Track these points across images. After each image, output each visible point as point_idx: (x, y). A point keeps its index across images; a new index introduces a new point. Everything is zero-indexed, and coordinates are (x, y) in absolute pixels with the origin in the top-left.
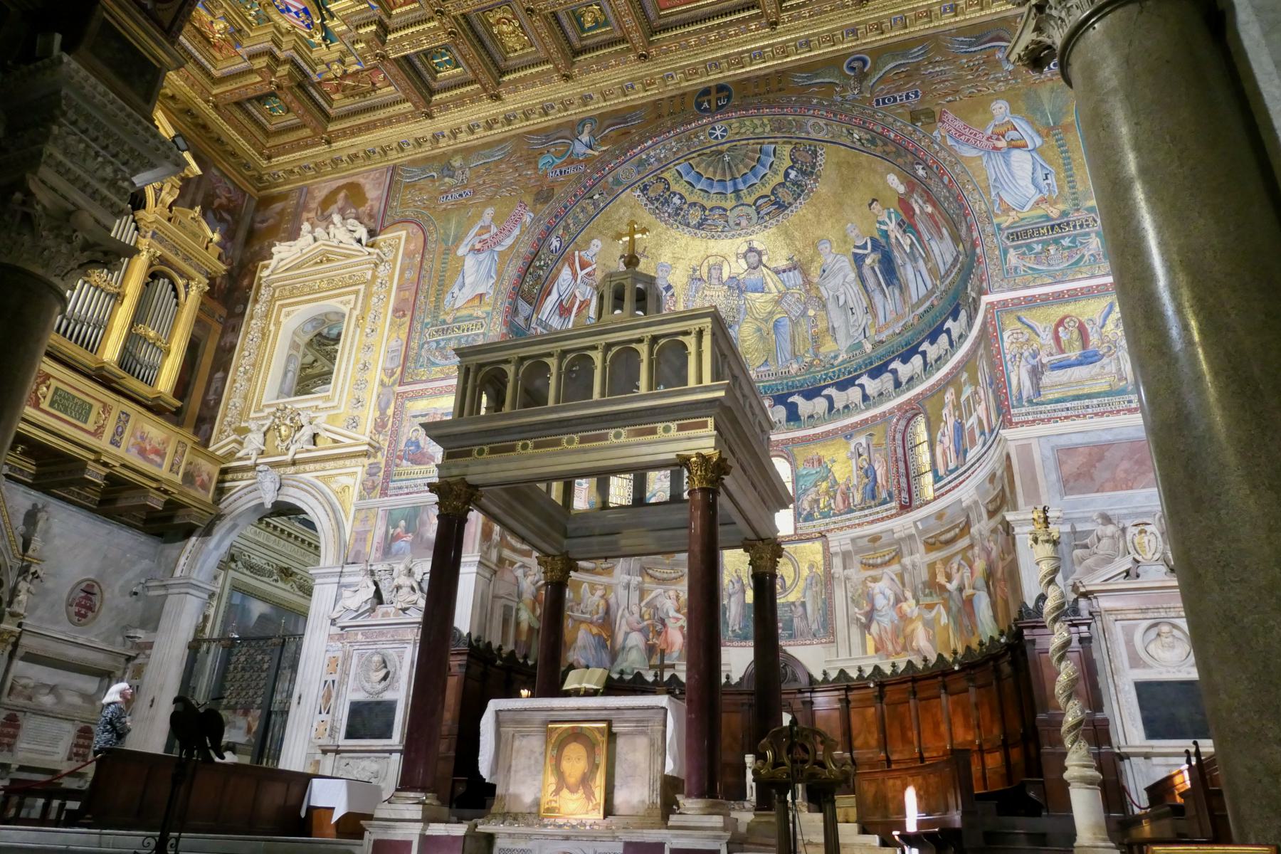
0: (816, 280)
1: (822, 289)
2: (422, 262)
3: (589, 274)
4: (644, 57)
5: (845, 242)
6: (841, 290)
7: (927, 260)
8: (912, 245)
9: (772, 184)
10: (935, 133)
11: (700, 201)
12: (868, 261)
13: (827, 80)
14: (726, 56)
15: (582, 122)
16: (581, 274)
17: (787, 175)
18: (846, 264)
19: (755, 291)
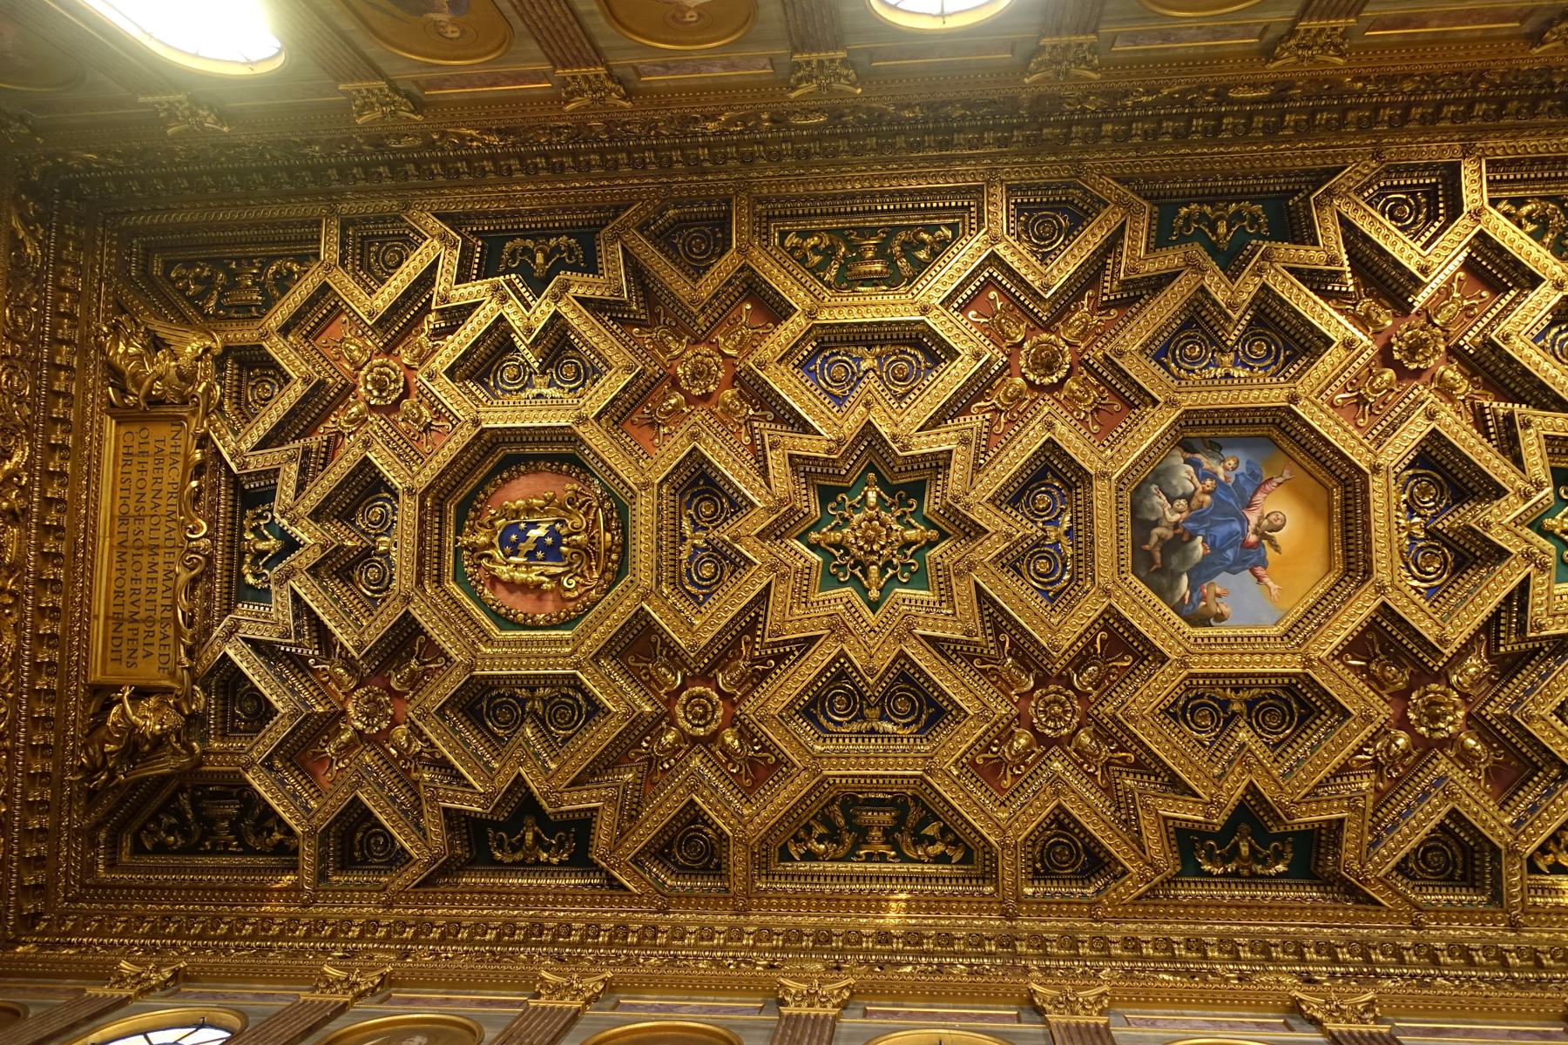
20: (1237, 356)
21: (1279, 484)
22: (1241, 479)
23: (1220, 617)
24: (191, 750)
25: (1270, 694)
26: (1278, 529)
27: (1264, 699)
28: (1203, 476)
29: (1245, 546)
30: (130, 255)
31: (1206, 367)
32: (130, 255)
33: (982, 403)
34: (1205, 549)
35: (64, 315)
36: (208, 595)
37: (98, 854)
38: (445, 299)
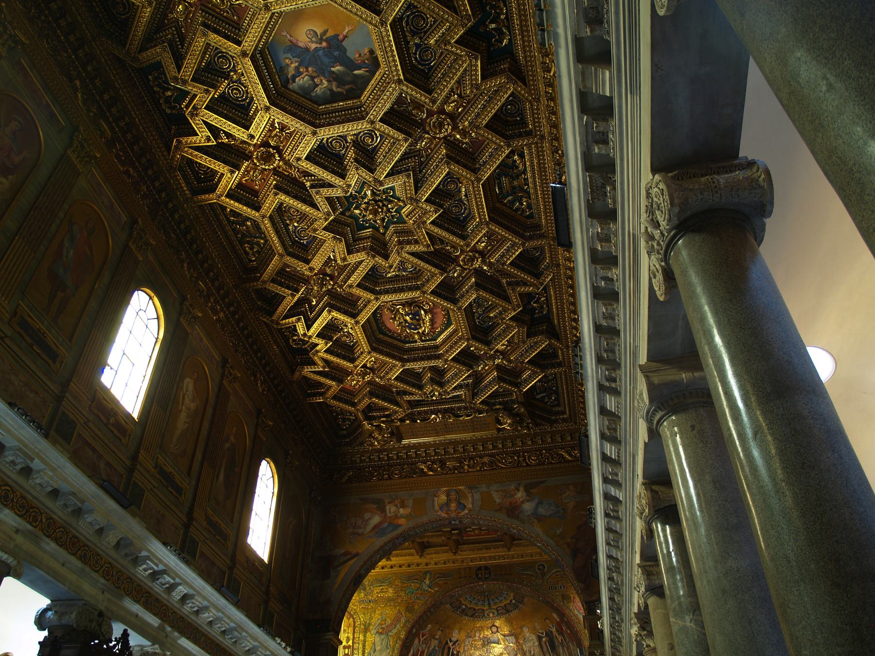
0: (521, 642)
1: (524, 646)
2: (354, 635)
3: (425, 639)
4: (455, 553)
5: (534, 629)
6: (532, 648)
7: (568, 648)
8: (562, 640)
9: (504, 603)
10: (571, 607)
11: (474, 607)
12: (544, 639)
13: (529, 573)
14: (488, 556)
15: (426, 573)
16: (422, 639)
17: (511, 601)
18: (534, 637)
19: (494, 643)
20: (231, 71)
21: (291, 36)
22: (294, 55)
23: (372, 52)
24: (516, 408)
25: (407, 25)
26: (315, 32)
27: (410, 28)
28: (298, 74)
29: (330, 46)
30: (342, 442)
31: (242, 84)
32: (342, 442)
33: (297, 176)
34: (337, 66)
35: (370, 459)
36: (459, 409)
37: (560, 418)
38: (324, 367)
